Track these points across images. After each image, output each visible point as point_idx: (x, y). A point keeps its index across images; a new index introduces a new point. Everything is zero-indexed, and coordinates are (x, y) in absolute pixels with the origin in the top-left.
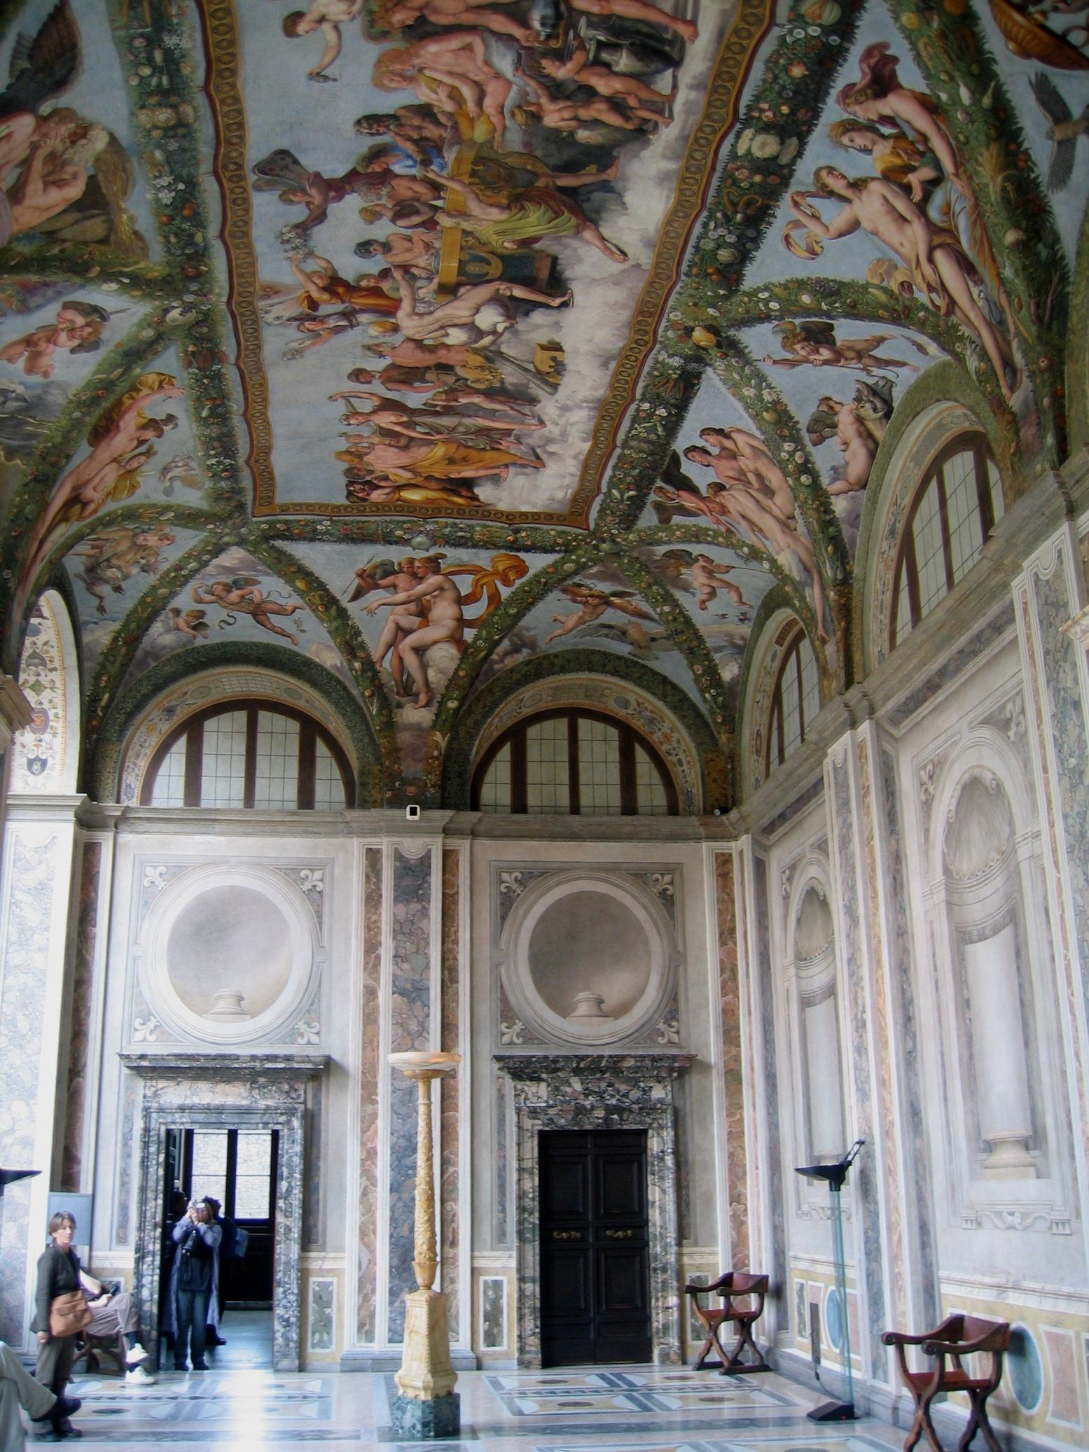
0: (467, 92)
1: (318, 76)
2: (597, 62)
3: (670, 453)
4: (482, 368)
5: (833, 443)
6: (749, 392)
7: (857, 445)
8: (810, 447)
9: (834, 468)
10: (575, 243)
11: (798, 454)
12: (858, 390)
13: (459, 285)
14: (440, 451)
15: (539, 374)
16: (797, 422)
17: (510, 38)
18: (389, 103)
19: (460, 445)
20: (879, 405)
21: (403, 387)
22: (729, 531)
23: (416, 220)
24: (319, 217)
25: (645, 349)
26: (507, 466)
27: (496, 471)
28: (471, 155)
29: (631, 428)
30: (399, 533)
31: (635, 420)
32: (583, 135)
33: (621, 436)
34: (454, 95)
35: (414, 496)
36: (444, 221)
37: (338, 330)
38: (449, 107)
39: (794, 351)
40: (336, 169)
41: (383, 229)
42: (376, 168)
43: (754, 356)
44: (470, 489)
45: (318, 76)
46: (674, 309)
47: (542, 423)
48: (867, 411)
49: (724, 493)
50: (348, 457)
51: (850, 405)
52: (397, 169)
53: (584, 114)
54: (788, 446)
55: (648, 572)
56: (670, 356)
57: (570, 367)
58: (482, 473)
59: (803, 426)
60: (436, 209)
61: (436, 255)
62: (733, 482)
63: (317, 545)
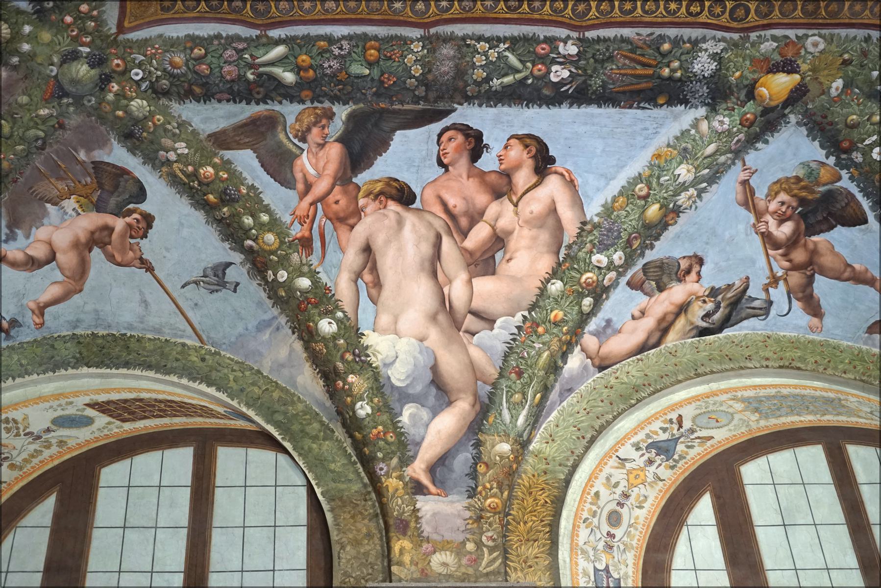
3: (441, 106)
5: (640, 299)
6: (684, 172)
7: (649, 323)
8: (624, 280)
9: (609, 322)
11: (613, 275)
12: (729, 287)
16: (652, 247)
20: (717, 316)
22: (306, 243)
25: (724, 20)
29: (494, 41)
31: (514, 42)
33: (460, 30)
39: (772, 194)
43: (751, 158)
46: (829, 40)
48: (697, 312)
49: (393, 206)
51: (701, 289)
54: (618, 257)
55: (28, 154)
56: (714, 56)
59: (651, 256)
62: (438, 210)
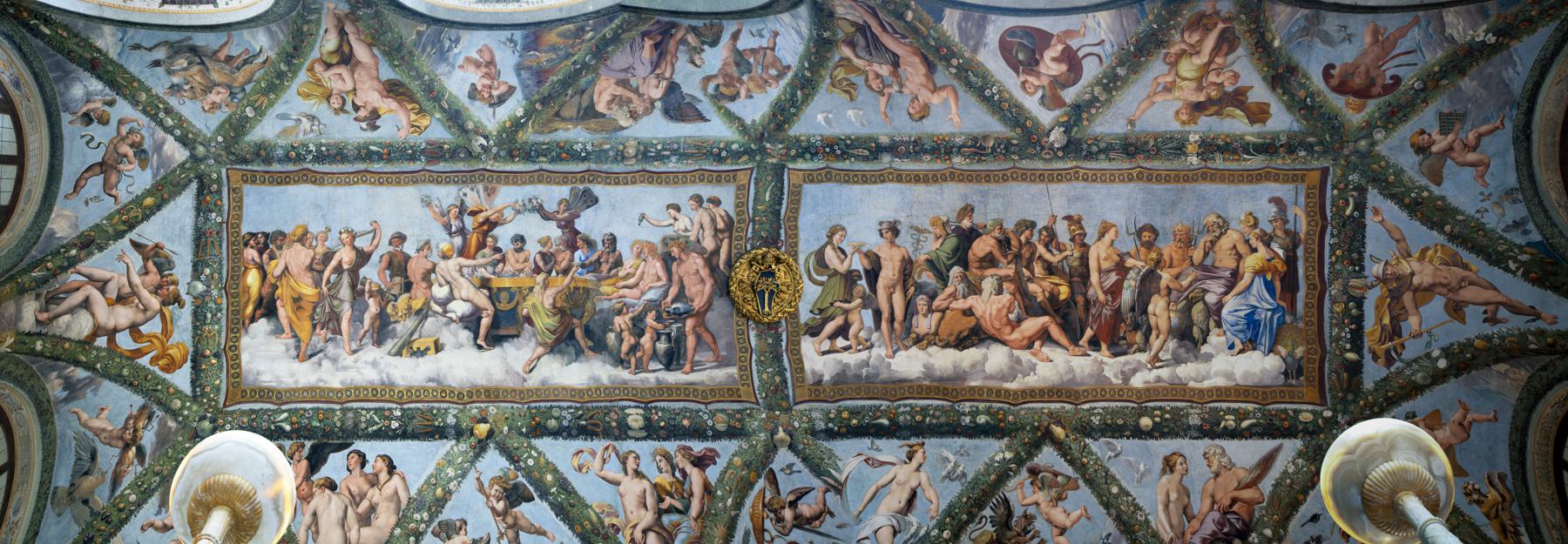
0: (632, 281)
1: (643, 217)
2: (659, 336)
4: (410, 308)
10: (533, 344)
13: (490, 289)
14: (309, 291)
15: (408, 344)
17: (665, 295)
18: (623, 247)
19: (315, 306)
21: (384, 264)
23: (541, 264)
24: (546, 216)
26: (295, 336)
27: (287, 329)
28: (590, 286)
30: (207, 271)
32: (611, 337)
34: (628, 276)
35: (253, 278)
36: (540, 278)
37: (447, 227)
38: (621, 274)
40: (580, 225)
41: (533, 249)
42: (580, 243)
44: (263, 316)
45: (643, 217)
47: (354, 352)
50: (299, 232)
52: (578, 254)
53: (625, 334)
57: (421, 360)
58: (284, 322)
60: (549, 273)
61: (513, 275)
63: (192, 213)
